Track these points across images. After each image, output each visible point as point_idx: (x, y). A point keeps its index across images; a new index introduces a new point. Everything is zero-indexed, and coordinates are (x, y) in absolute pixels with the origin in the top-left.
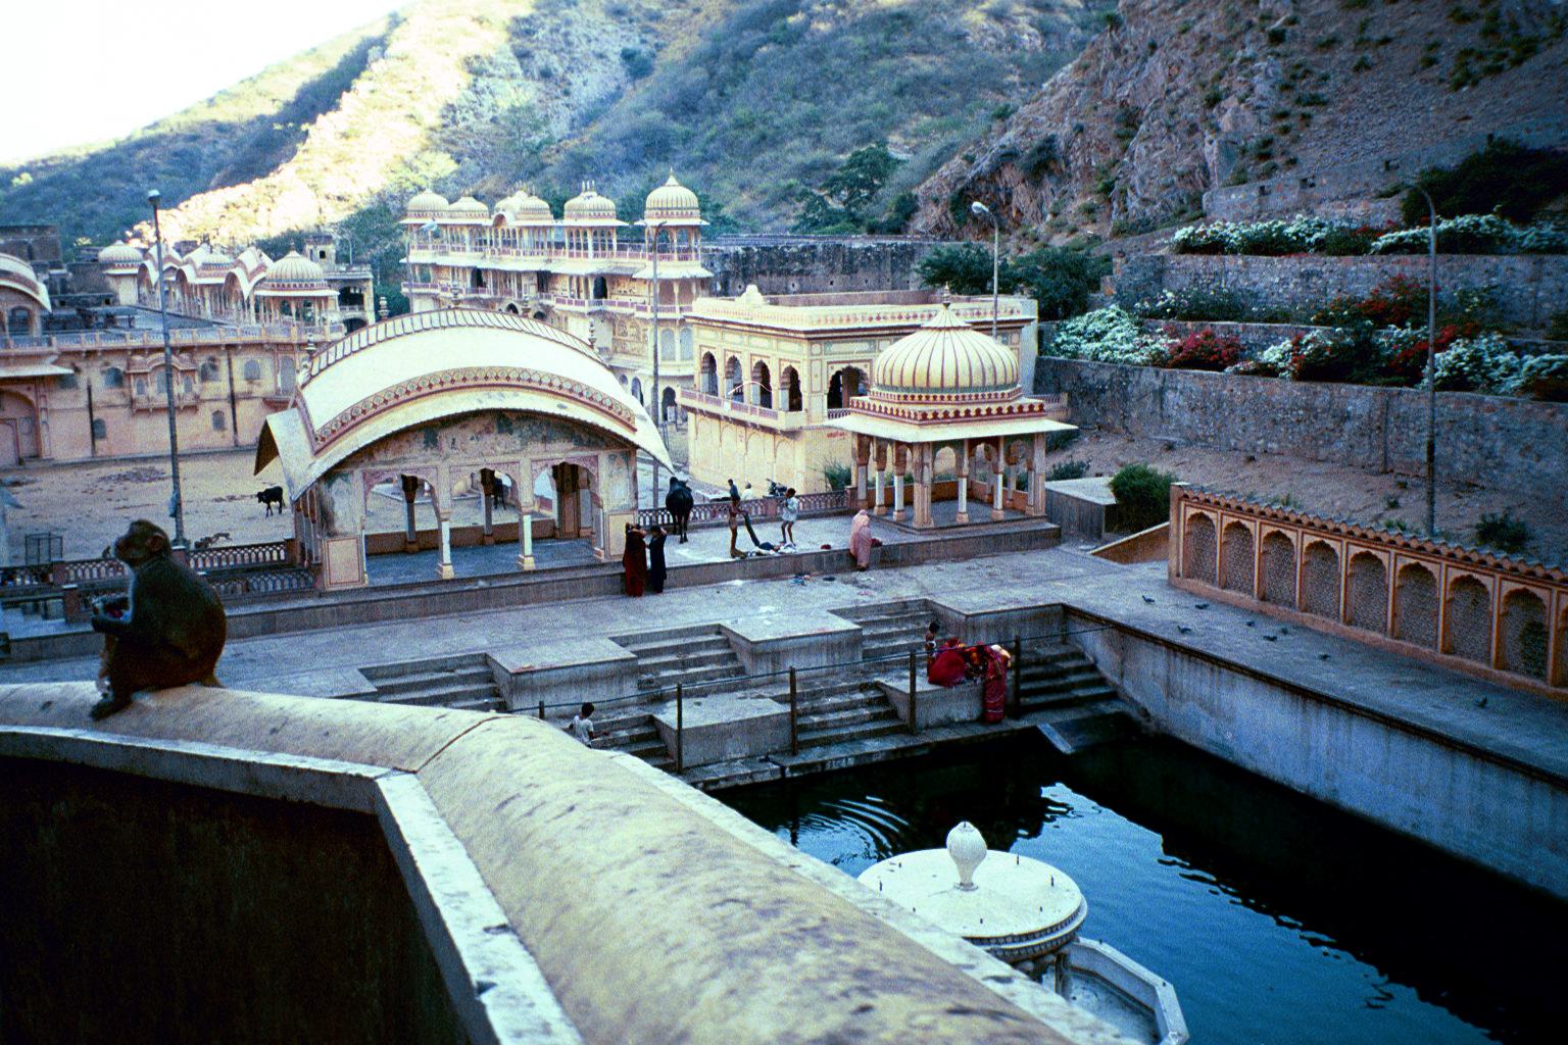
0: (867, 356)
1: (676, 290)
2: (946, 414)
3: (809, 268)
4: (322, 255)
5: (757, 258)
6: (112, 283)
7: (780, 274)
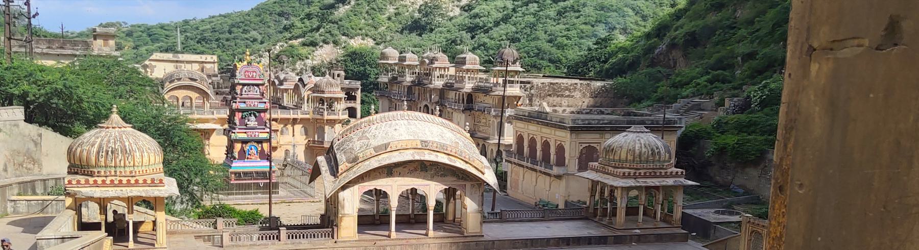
3: (573, 94)
4: (338, 76)
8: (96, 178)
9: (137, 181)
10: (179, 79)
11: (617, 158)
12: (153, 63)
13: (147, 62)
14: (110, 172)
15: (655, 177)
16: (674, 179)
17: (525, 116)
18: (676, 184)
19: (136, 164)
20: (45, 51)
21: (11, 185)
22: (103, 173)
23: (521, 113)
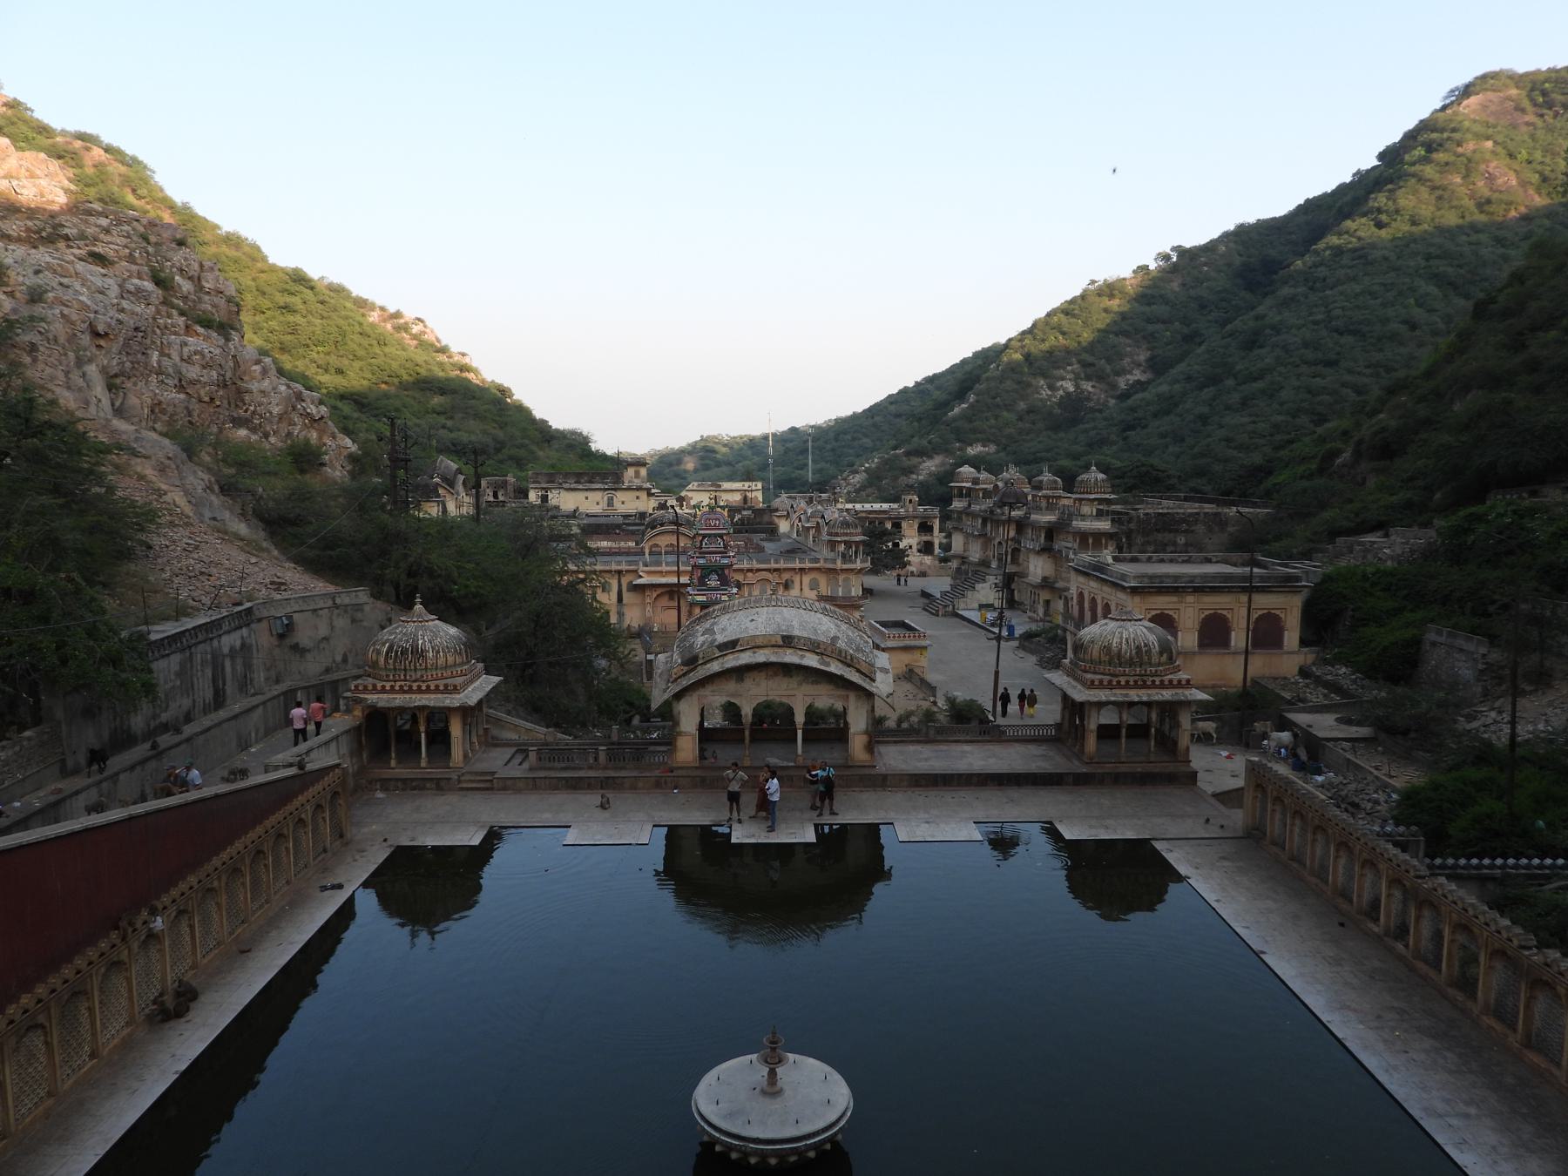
0: (1177, 606)
1: (1090, 541)
2: (1101, 682)
3: (1193, 528)
4: (910, 501)
5: (1153, 521)
6: (776, 520)
7: (1170, 531)
8: (384, 683)
9: (428, 687)
10: (662, 525)
11: (1088, 657)
12: (690, 494)
13: (683, 494)
14: (399, 676)
15: (1144, 686)
16: (1174, 691)
17: (1084, 567)
18: (1176, 698)
19: (429, 666)
20: (572, 486)
21: (345, 679)
22: (391, 677)
23: (1081, 563)
